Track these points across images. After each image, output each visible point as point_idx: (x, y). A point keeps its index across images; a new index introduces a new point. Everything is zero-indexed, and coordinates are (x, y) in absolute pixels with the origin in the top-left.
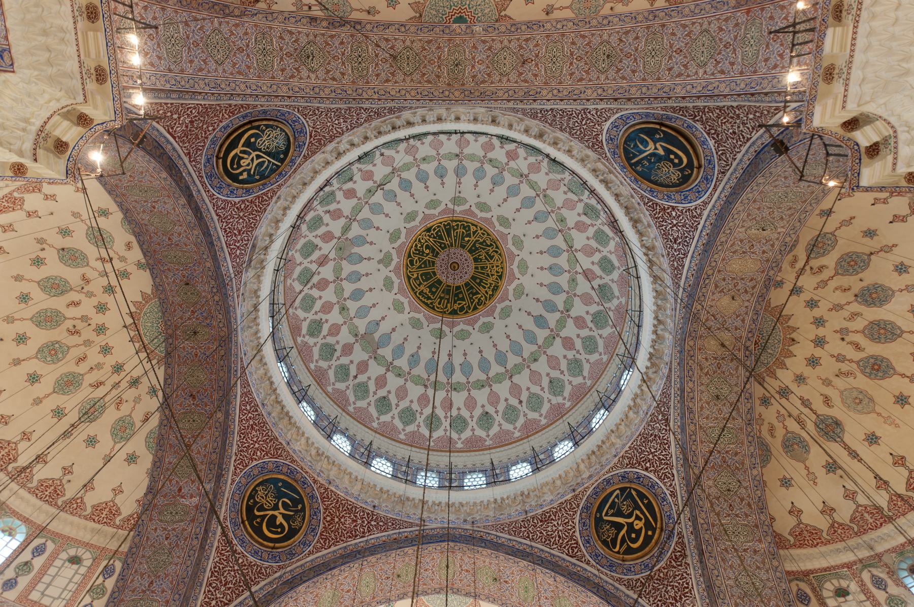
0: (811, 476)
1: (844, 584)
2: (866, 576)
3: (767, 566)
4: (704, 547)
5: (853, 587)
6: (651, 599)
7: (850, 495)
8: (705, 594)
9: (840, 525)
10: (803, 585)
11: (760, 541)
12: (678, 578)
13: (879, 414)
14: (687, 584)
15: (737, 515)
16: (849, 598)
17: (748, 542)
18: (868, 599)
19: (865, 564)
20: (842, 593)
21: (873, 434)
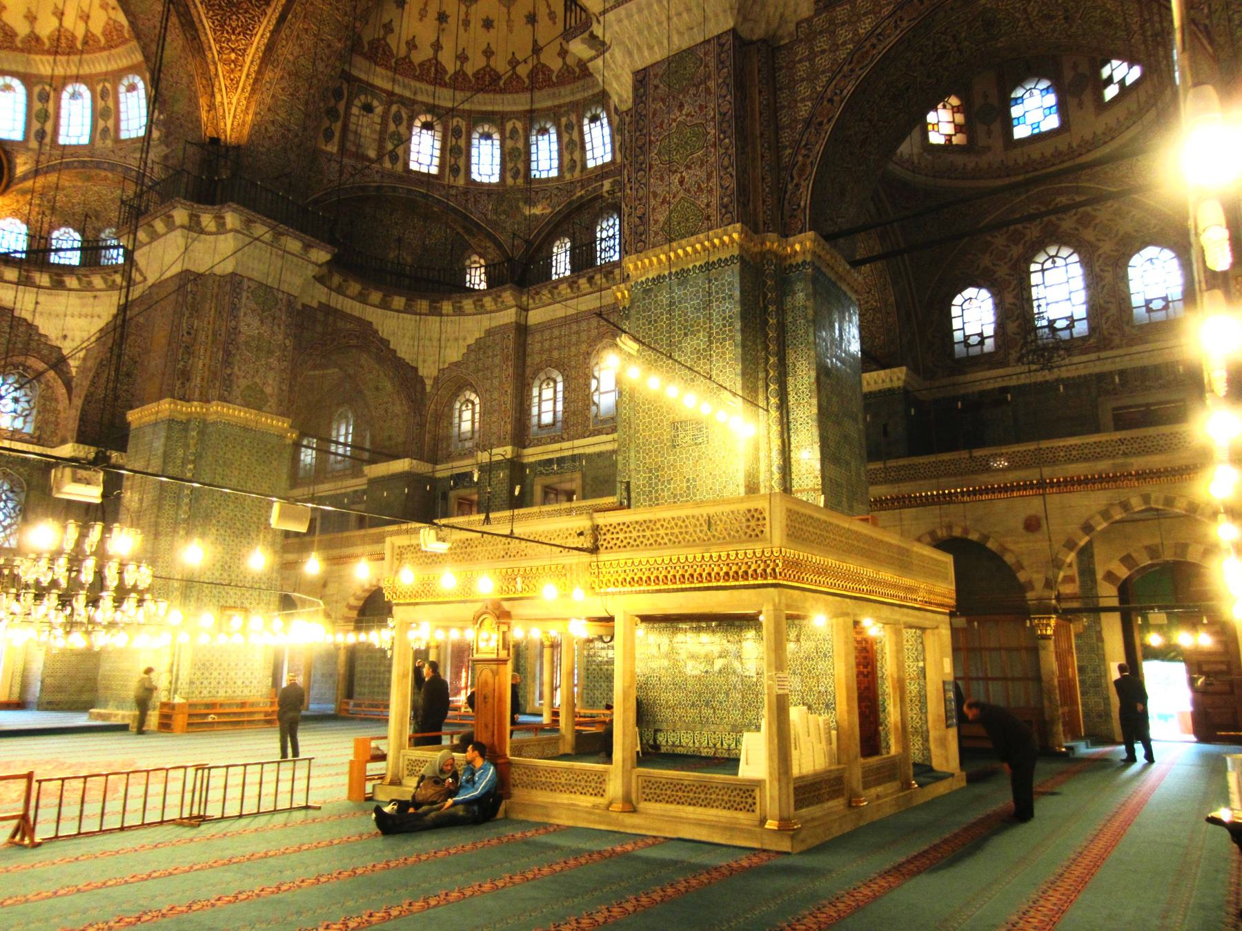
0: (423, 12)
1: (375, 103)
2: (394, 108)
3: (330, 62)
4: (290, 16)
5: (379, 110)
6: (211, 13)
7: (437, 46)
8: (263, 48)
9: (411, 62)
10: (345, 86)
11: (340, 40)
12: (248, 15)
13: (509, 13)
14: (254, 28)
15: (338, 9)
16: (371, 115)
17: (331, 35)
18: (381, 124)
19: (402, 101)
20: (368, 108)
21: (492, 21)
